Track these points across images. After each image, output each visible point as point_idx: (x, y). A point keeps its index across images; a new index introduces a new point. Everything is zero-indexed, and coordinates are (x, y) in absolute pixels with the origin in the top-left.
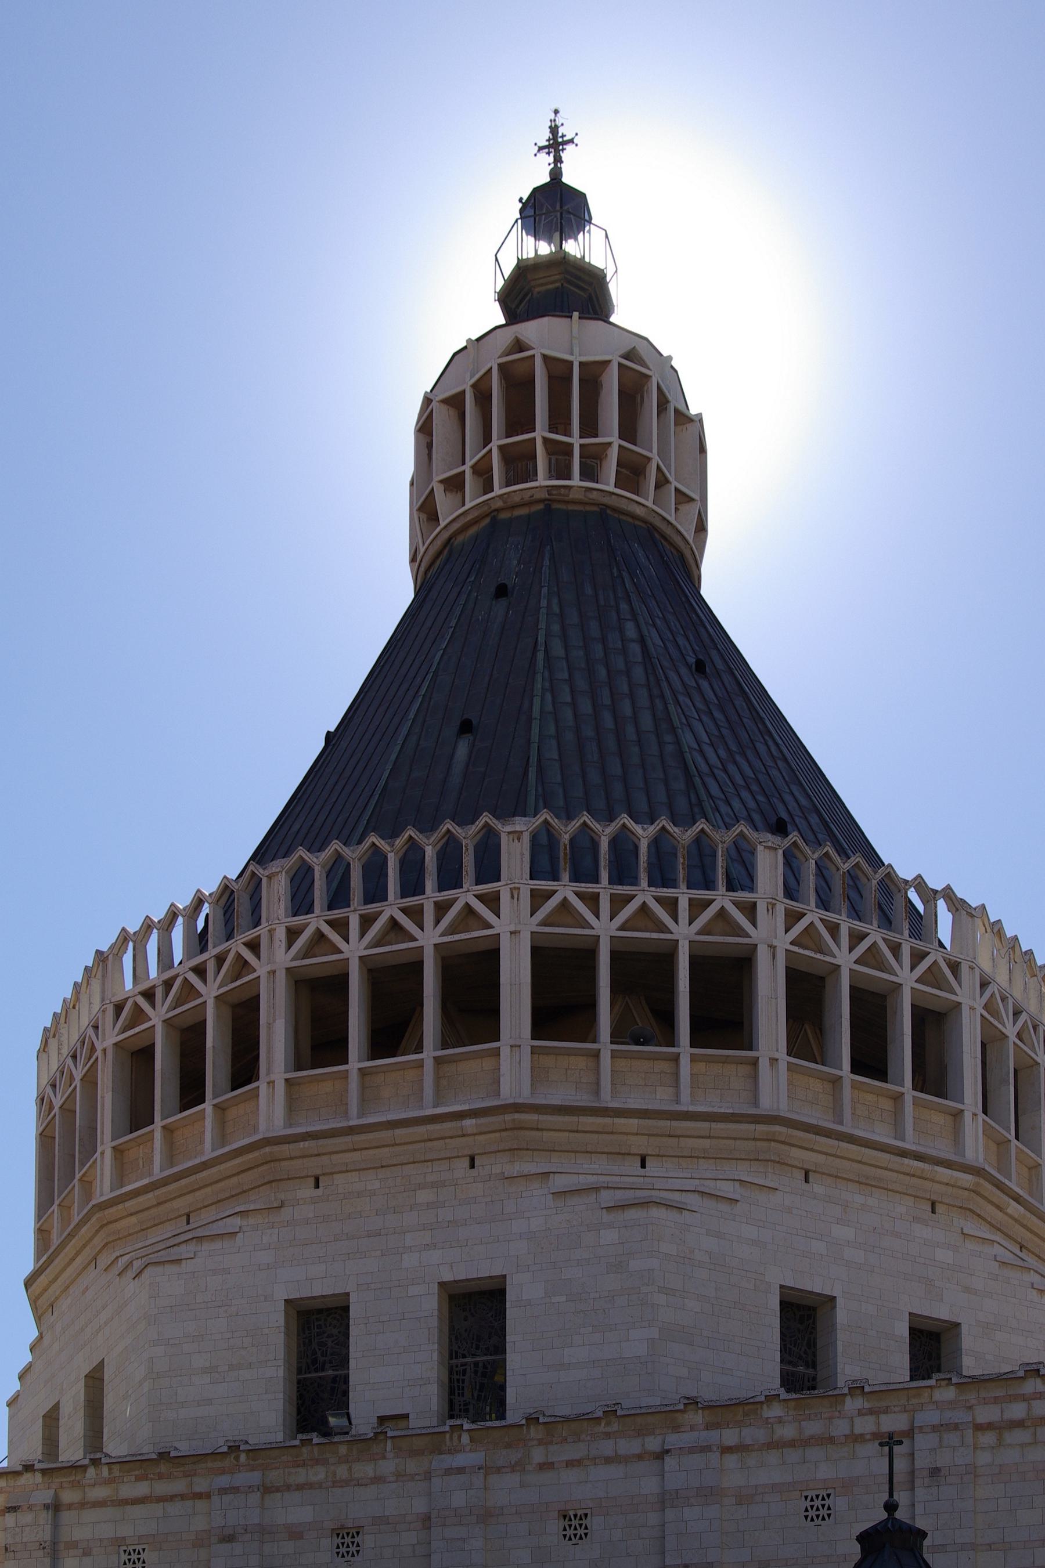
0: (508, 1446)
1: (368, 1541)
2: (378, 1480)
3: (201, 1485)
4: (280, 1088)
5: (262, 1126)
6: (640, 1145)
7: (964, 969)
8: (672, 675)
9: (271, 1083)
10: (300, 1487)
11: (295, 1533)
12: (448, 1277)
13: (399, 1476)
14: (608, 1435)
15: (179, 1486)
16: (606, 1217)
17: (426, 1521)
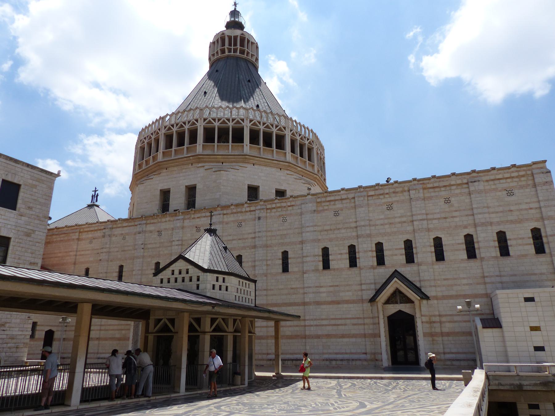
0: (188, 215)
1: (163, 233)
2: (166, 221)
3: (136, 223)
4: (161, 153)
5: (158, 160)
6: (222, 160)
7: (286, 128)
8: (243, 83)
9: (160, 152)
10: (153, 223)
11: (151, 232)
12: (187, 184)
13: (169, 221)
14: (204, 212)
15: (133, 224)
16: (214, 173)
17: (173, 229)
